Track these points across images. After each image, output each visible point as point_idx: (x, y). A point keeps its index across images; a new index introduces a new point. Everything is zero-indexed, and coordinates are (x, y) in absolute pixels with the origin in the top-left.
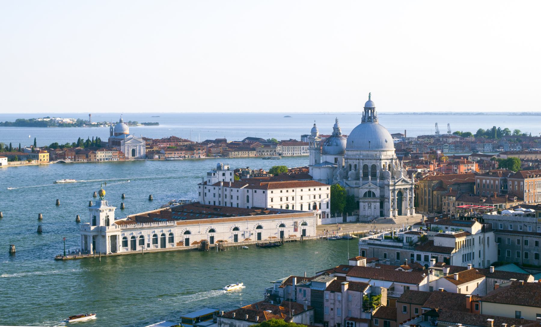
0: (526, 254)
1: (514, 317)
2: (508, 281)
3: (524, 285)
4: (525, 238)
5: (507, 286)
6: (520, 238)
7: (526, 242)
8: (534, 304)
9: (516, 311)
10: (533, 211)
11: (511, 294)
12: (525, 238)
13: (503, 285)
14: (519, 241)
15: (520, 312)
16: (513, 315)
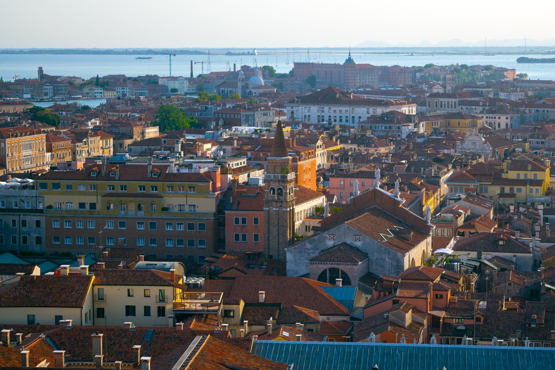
0: (25, 239)
1: (26, 323)
2: (16, 276)
3: (36, 280)
4: (22, 218)
5: (14, 283)
6: (16, 218)
7: (24, 223)
8: (51, 303)
9: (28, 315)
10: (31, 181)
11: (20, 293)
12: (22, 218)
13: (6, 283)
14: (14, 221)
15: (34, 316)
16: (26, 323)
